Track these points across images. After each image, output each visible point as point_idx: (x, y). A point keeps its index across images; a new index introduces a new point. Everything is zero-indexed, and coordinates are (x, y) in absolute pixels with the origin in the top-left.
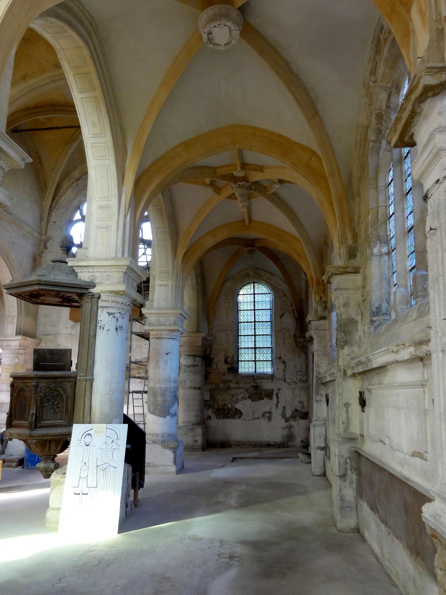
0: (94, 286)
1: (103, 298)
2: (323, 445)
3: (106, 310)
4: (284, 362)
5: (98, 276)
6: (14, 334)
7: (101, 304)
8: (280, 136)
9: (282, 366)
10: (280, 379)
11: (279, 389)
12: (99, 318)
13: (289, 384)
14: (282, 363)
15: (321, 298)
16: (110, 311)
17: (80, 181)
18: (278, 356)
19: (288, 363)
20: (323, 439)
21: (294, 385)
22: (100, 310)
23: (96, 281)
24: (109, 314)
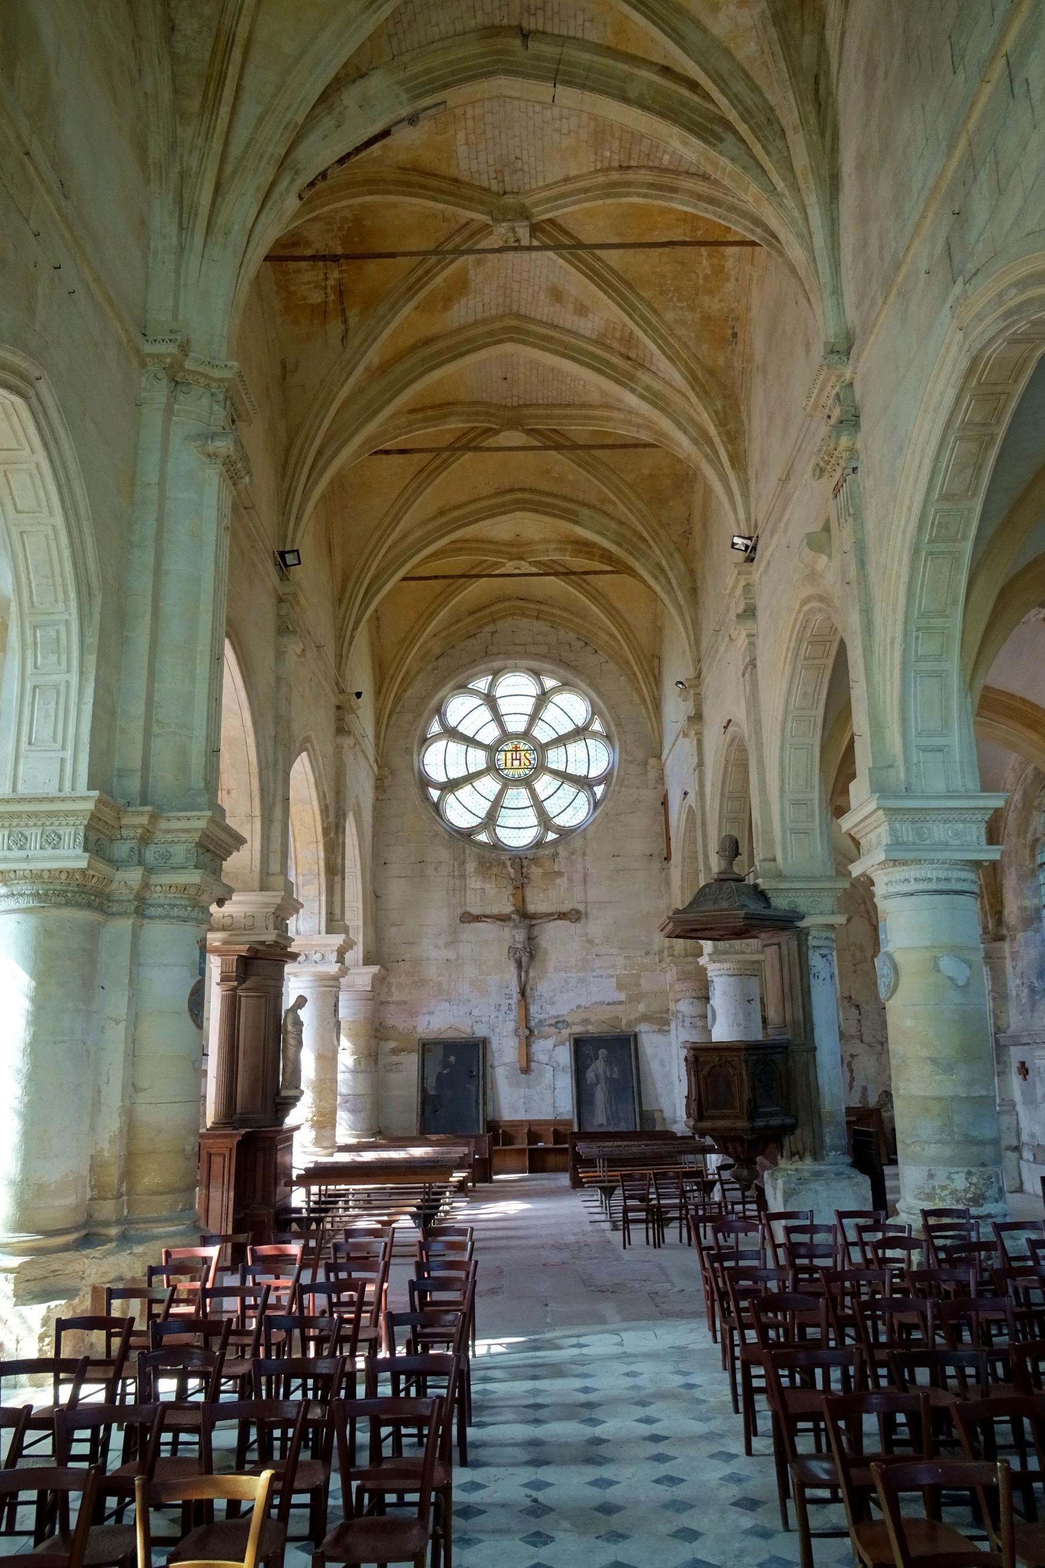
0: (802, 918)
1: (813, 933)
2: (1015, 1144)
3: (819, 951)
4: (857, 1006)
5: (802, 904)
6: (361, 962)
7: (812, 942)
8: (1024, 701)
9: (854, 1013)
10: (852, 1037)
11: (852, 1056)
12: (811, 963)
13: (870, 1045)
14: (853, 1009)
15: (991, 907)
16: (824, 952)
17: (440, 660)
18: (847, 995)
19: (865, 1008)
20: (1013, 1134)
21: (879, 1047)
22: (810, 952)
23: (802, 909)
24: (823, 956)
